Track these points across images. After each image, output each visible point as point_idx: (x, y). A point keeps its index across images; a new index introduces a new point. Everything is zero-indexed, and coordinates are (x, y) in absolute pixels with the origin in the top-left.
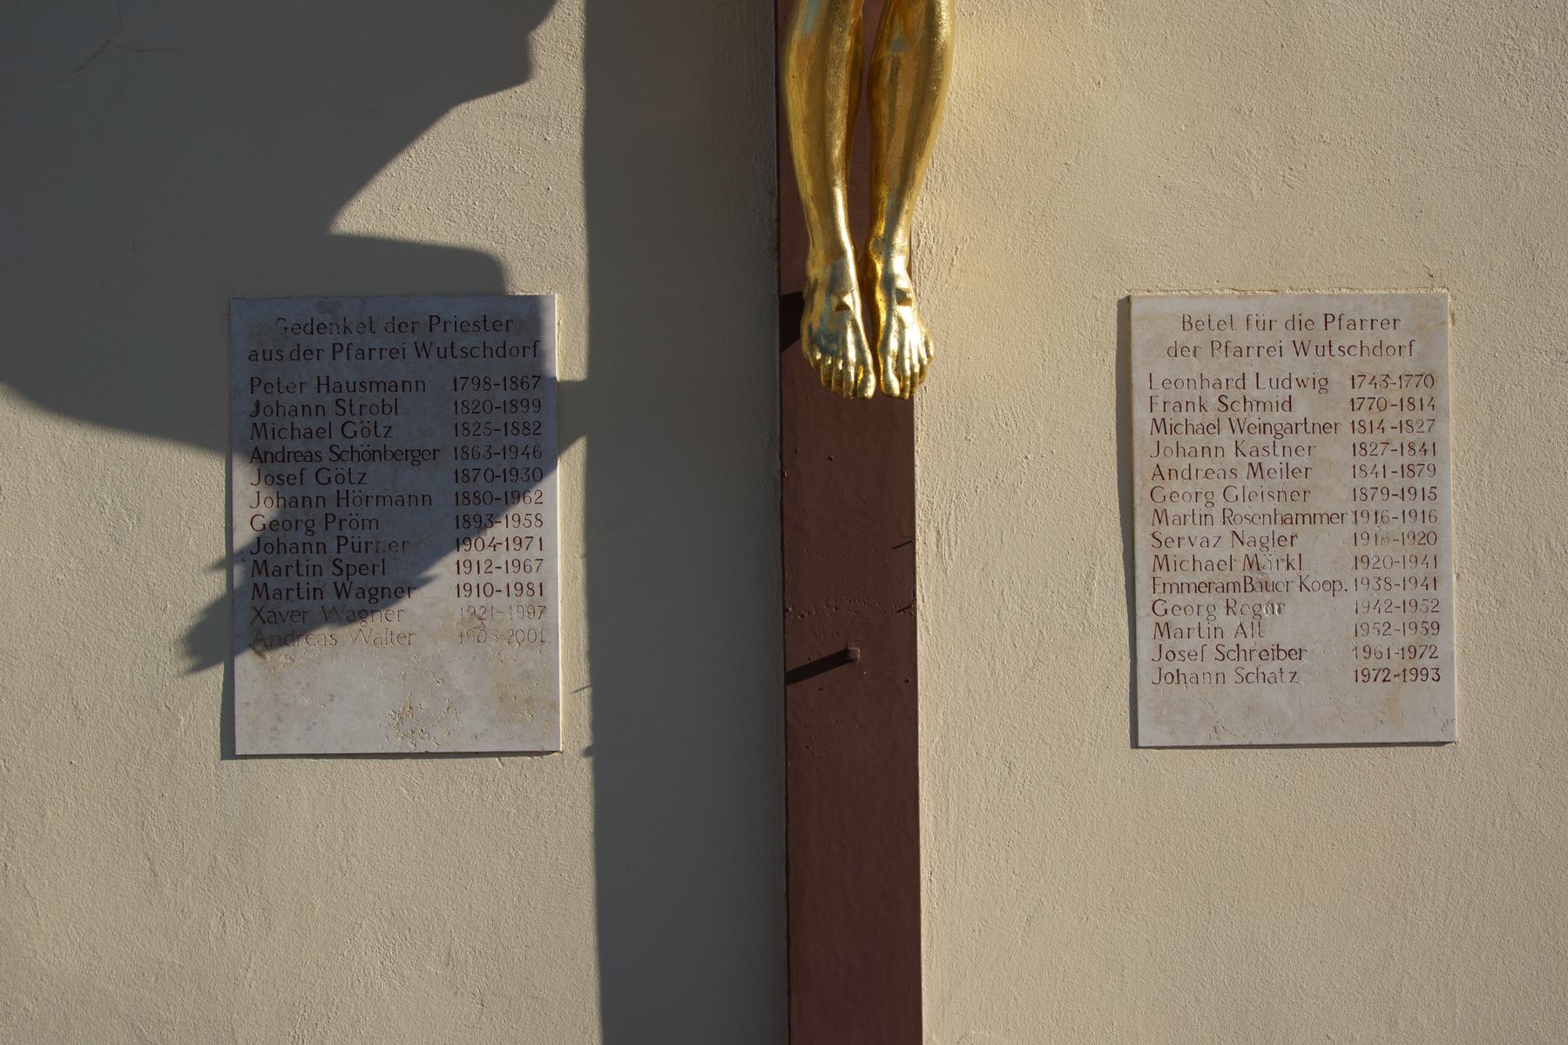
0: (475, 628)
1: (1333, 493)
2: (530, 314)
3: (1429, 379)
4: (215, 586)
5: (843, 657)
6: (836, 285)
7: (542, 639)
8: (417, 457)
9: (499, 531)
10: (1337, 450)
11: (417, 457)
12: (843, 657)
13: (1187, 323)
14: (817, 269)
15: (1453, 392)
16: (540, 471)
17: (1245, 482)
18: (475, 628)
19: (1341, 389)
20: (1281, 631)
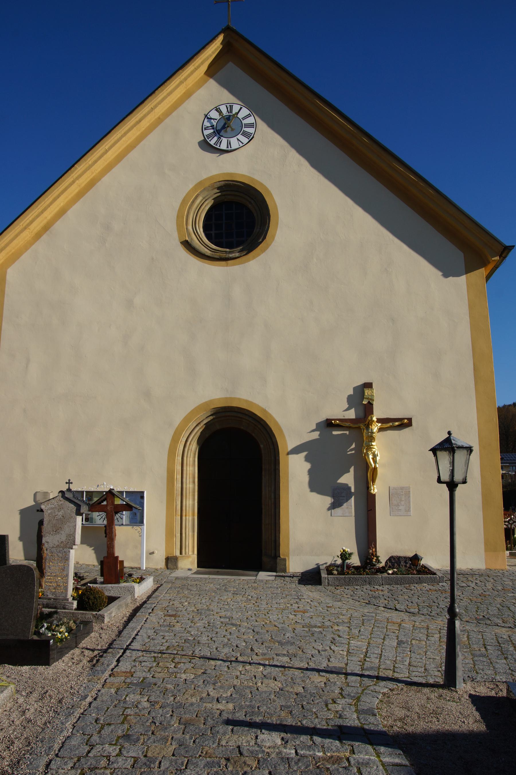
0: (347, 508)
1: (403, 499)
2: (350, 488)
3: (409, 492)
4: (329, 505)
5: (371, 510)
6: (371, 487)
7: (352, 509)
8: (344, 497)
9: (349, 502)
10: (403, 496)
11: (344, 497)
12: (371, 510)
14: (370, 486)
15: (411, 492)
16: (352, 497)
17: (397, 498)
18: (347, 508)
19: (404, 492)
20: (400, 508)
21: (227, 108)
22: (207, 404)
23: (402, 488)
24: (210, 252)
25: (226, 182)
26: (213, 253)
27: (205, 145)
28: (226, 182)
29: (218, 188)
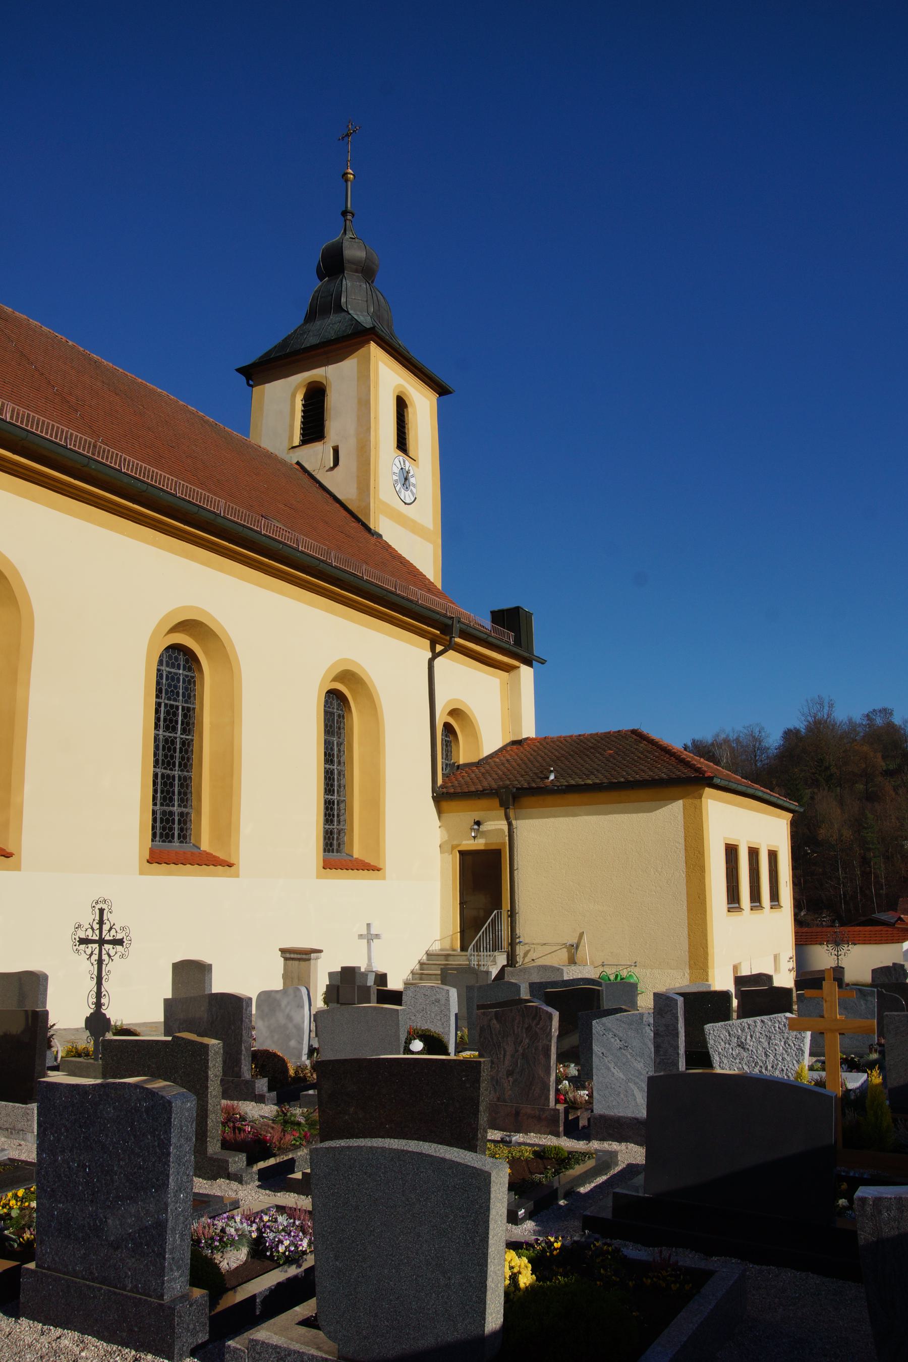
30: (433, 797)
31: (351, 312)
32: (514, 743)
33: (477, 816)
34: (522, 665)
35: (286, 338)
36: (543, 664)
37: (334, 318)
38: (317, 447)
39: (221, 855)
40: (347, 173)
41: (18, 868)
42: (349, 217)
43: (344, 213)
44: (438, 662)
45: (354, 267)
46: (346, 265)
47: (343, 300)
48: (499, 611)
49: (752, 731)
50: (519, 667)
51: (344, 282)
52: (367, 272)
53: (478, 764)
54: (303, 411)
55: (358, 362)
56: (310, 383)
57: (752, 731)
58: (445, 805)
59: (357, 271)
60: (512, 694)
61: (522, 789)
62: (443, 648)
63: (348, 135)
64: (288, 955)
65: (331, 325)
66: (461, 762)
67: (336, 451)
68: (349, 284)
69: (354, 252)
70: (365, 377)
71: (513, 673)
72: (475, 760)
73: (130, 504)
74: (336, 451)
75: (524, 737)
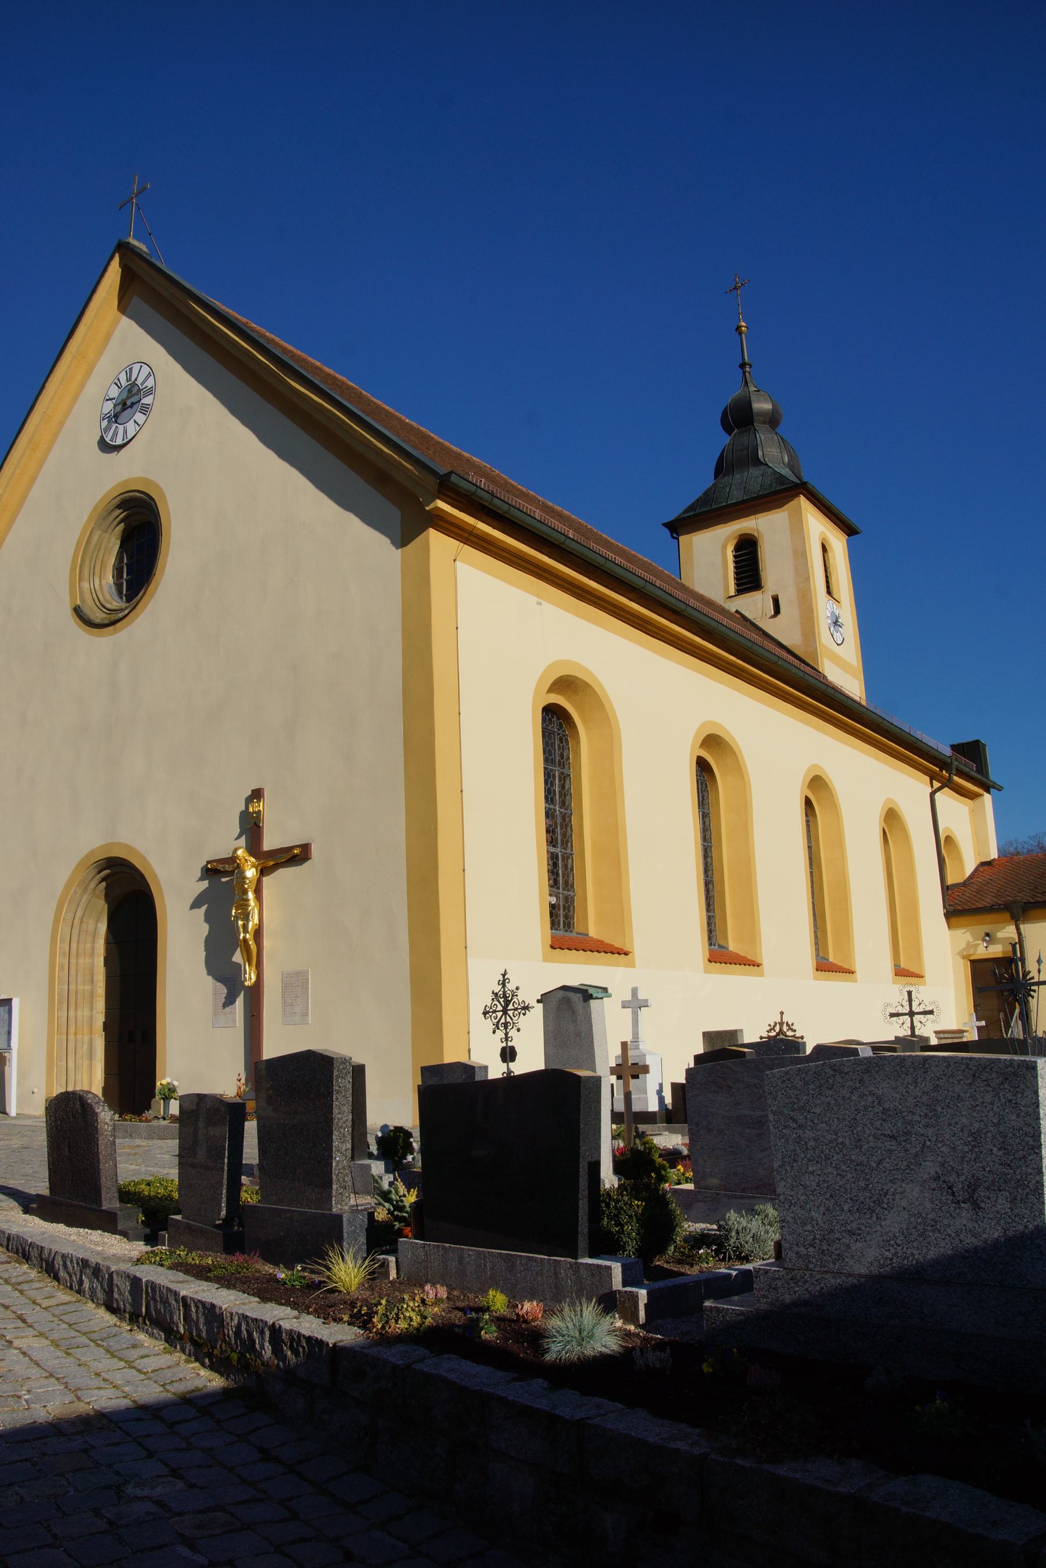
13: (288, 974)
21: (127, 374)
22: (87, 857)
23: (298, 974)
24: (104, 615)
25: (122, 496)
26: (109, 616)
27: (106, 447)
28: (122, 496)
29: (118, 507)
30: (944, 914)
31: (770, 465)
32: (983, 864)
33: (986, 928)
34: (985, 793)
35: (706, 492)
36: (1000, 790)
37: (754, 472)
38: (754, 597)
39: (846, 966)
40: (741, 326)
41: (762, 975)
42: (747, 369)
43: (743, 366)
44: (938, 796)
45: (762, 419)
46: (756, 418)
47: (760, 453)
48: (959, 745)
49: (1039, 842)
50: (983, 795)
51: (758, 436)
52: (773, 420)
53: (964, 884)
54: (735, 562)
55: (789, 515)
56: (741, 535)
57: (1039, 842)
58: (953, 920)
59: (764, 423)
60: (977, 818)
61: (1029, 903)
62: (940, 785)
63: (736, 288)
64: (942, 1035)
65: (752, 479)
66: (949, 884)
67: (776, 601)
68: (762, 437)
69: (762, 405)
70: (798, 527)
71: (978, 801)
72: (962, 881)
73: (788, 688)
74: (776, 601)
75: (992, 858)
